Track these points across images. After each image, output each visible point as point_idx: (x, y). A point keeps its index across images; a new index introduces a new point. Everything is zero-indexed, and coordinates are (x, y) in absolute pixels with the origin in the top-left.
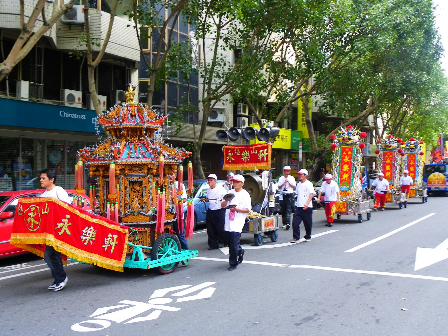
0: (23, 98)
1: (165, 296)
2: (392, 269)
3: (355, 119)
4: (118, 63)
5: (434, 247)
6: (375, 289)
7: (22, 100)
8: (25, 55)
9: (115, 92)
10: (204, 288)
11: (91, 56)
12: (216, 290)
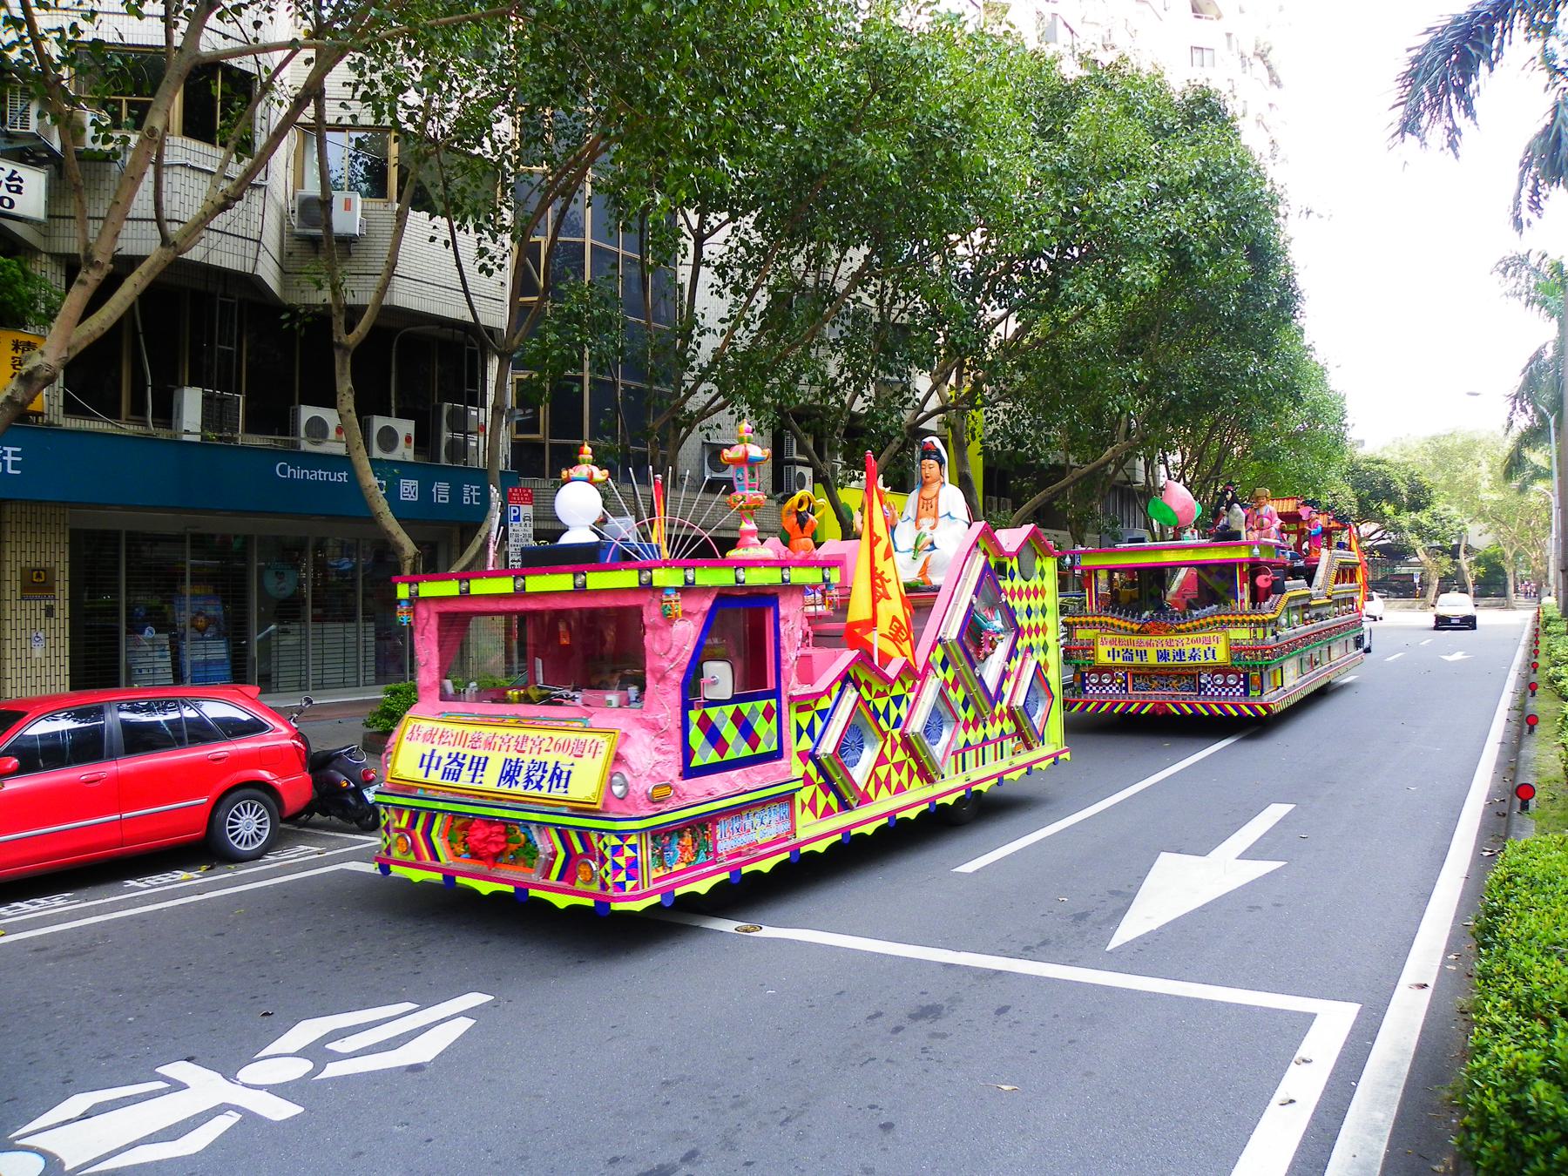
0: (187, 432)
1: (302, 1053)
2: (1044, 943)
3: (1087, 468)
4: (446, 333)
5: (1203, 852)
6: (944, 1036)
7: (186, 438)
8: (107, 327)
9: (440, 408)
10: (443, 1021)
11: (342, 319)
12: (468, 1031)
